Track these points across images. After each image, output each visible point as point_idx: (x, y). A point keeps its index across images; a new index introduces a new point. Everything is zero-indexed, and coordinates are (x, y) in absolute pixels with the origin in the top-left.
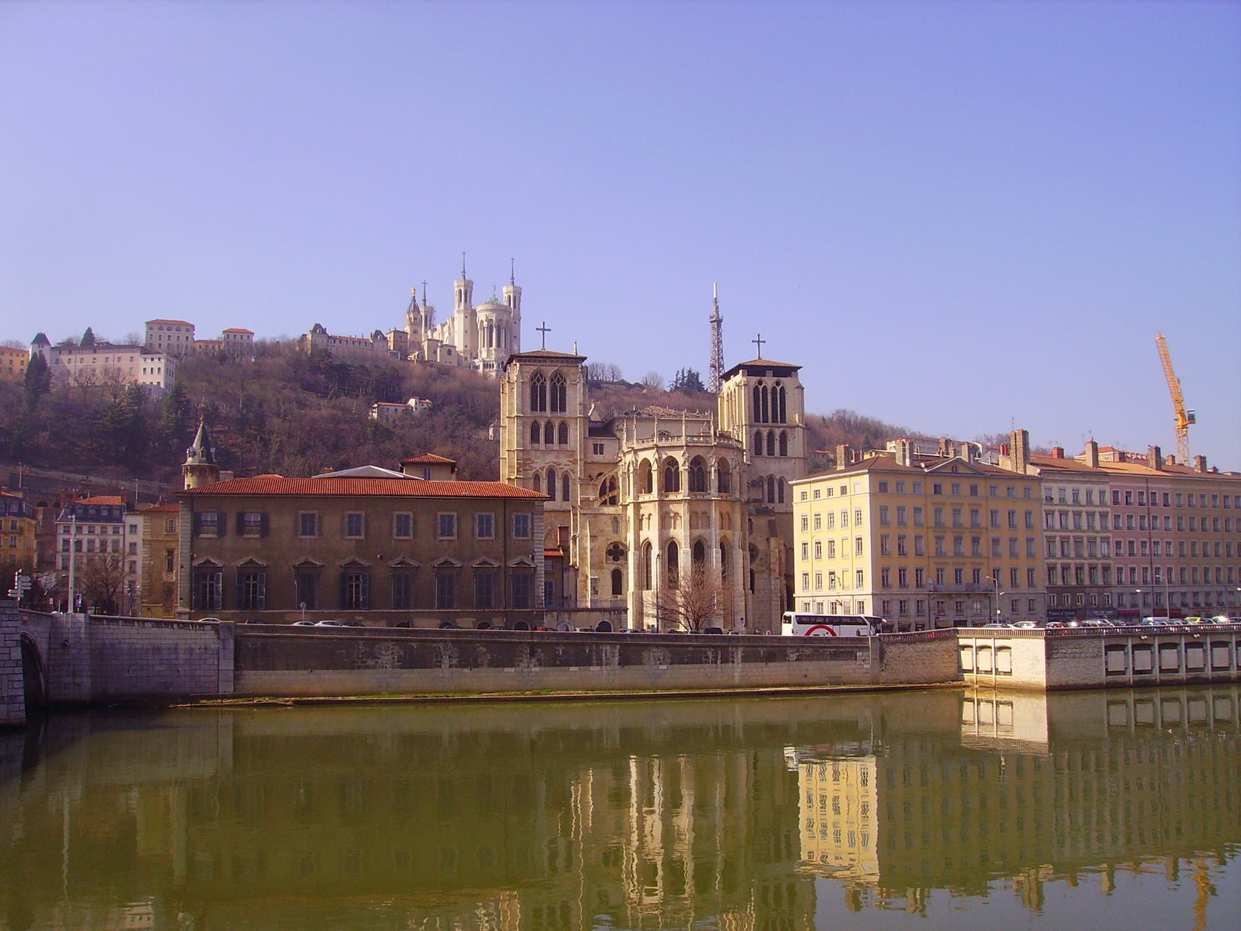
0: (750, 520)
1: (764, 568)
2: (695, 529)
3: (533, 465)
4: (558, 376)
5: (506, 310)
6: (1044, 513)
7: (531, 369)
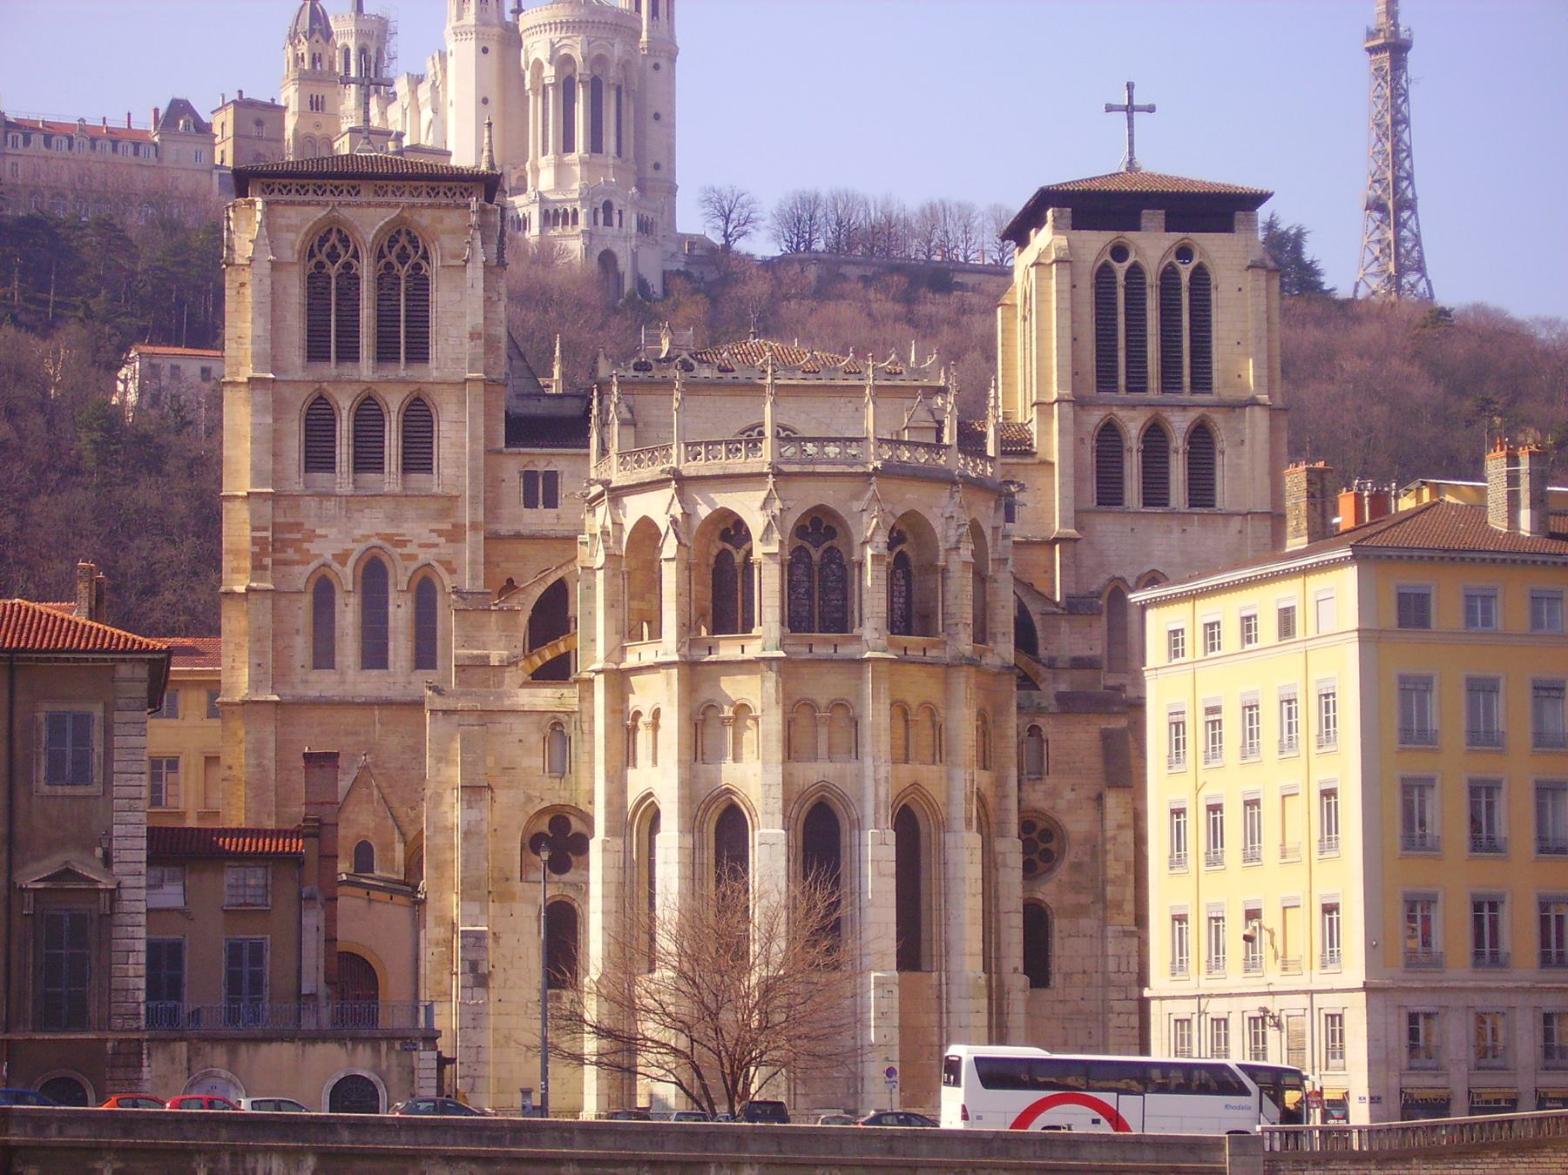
1: (1085, 899)
2: (809, 760)
3: (313, 547)
4: (403, 240)
5: (623, 26)
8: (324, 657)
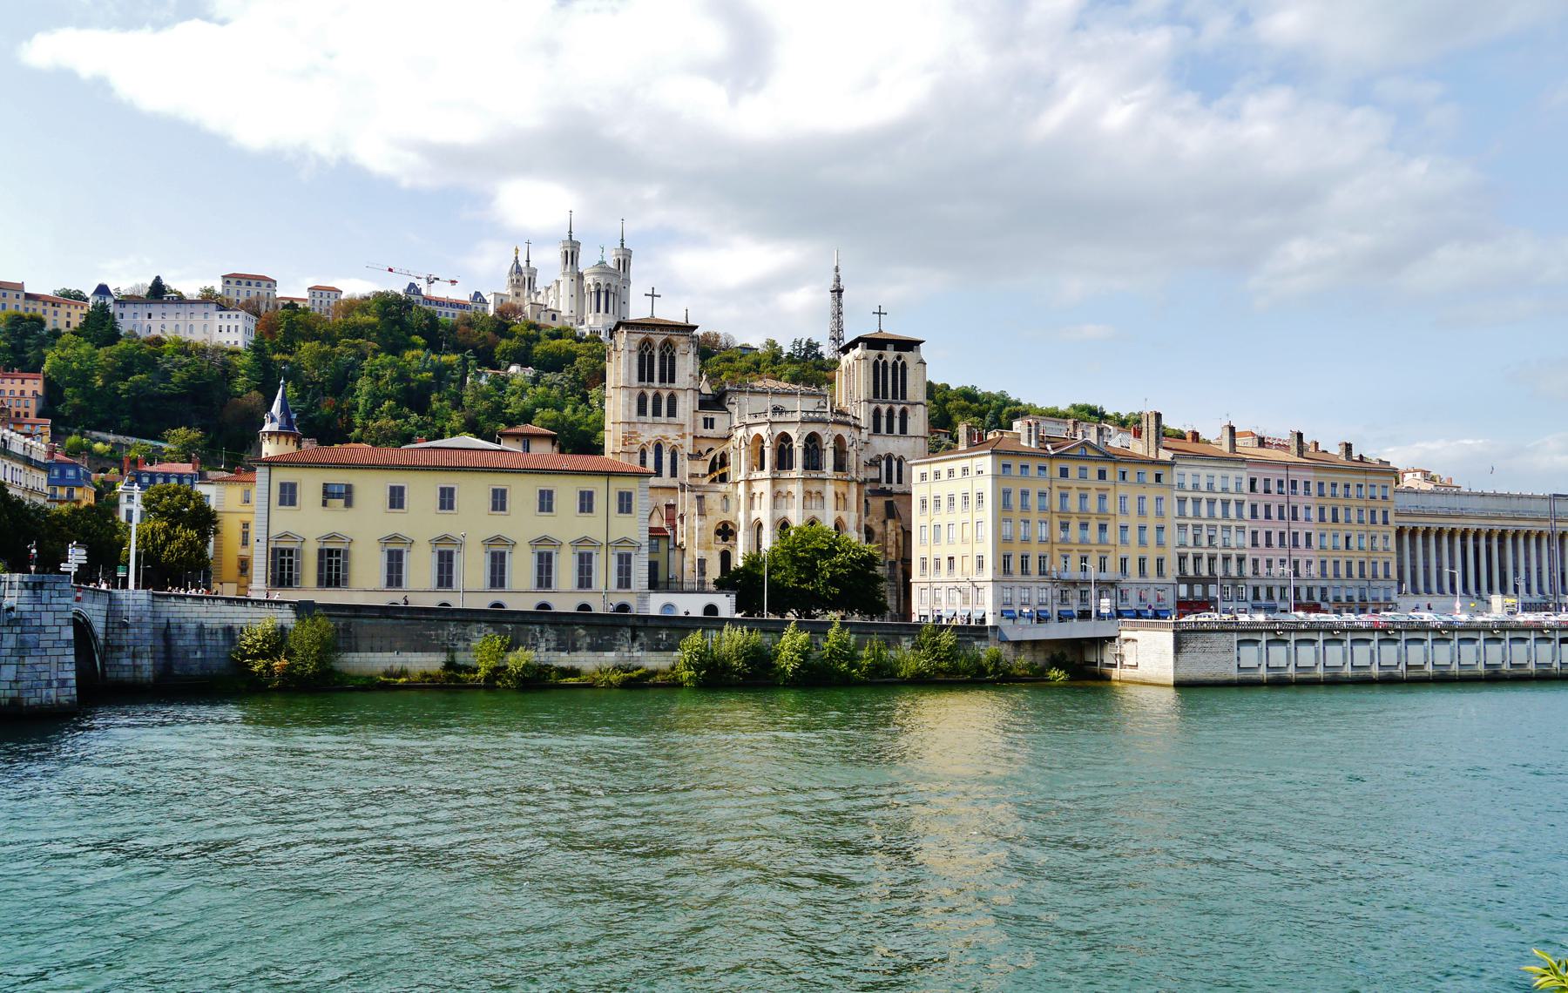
0: (866, 501)
3: (640, 439)
5: (614, 273)
6: (1176, 500)
7: (638, 337)
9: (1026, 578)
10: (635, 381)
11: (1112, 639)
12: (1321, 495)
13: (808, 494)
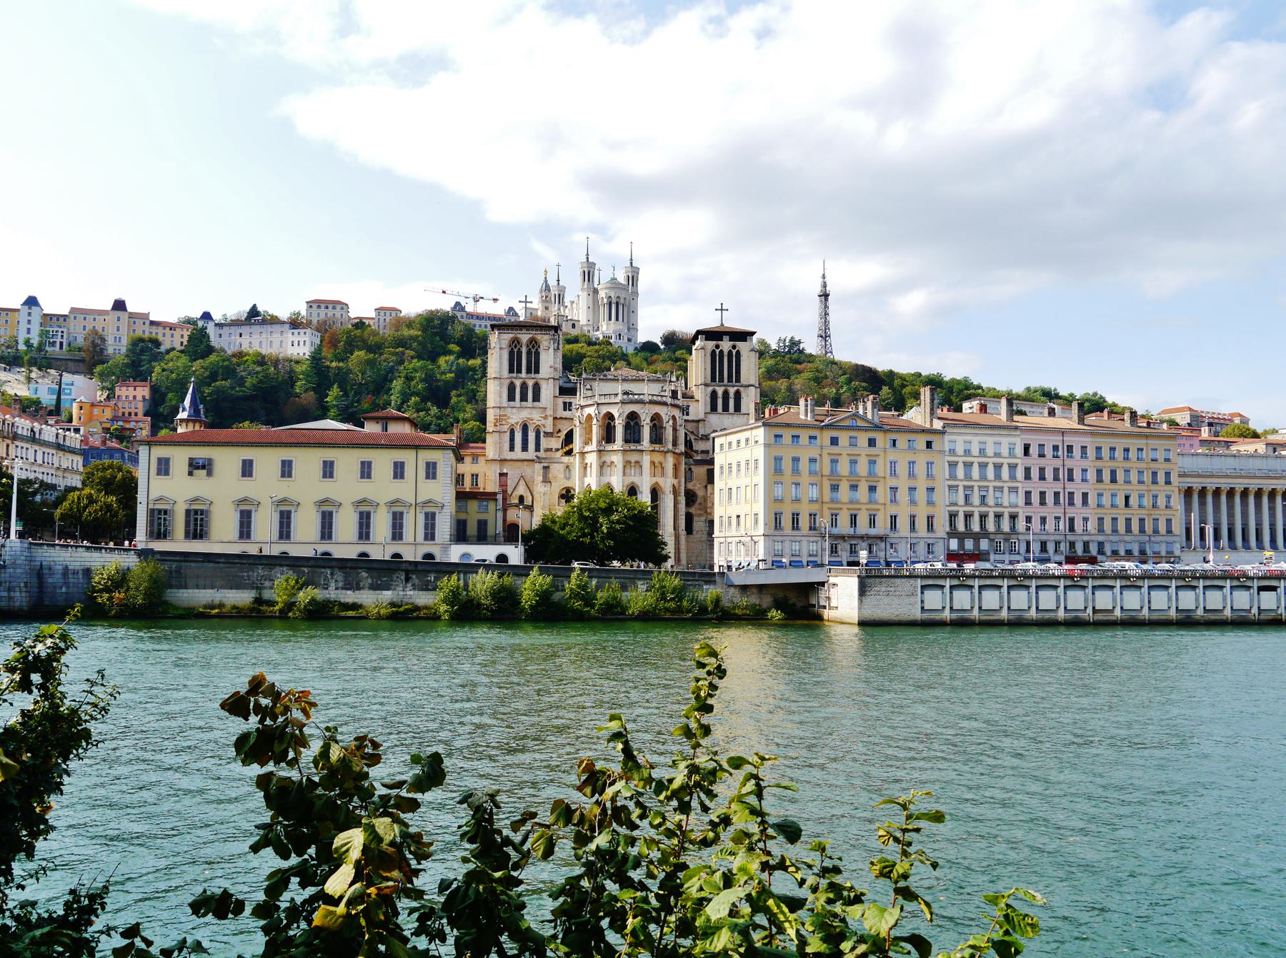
3: (510, 421)
5: (624, 288)
6: (947, 464)
8: (512, 448)
9: (796, 533)
10: (505, 373)
11: (822, 584)
12: (1099, 458)
13: (627, 464)
